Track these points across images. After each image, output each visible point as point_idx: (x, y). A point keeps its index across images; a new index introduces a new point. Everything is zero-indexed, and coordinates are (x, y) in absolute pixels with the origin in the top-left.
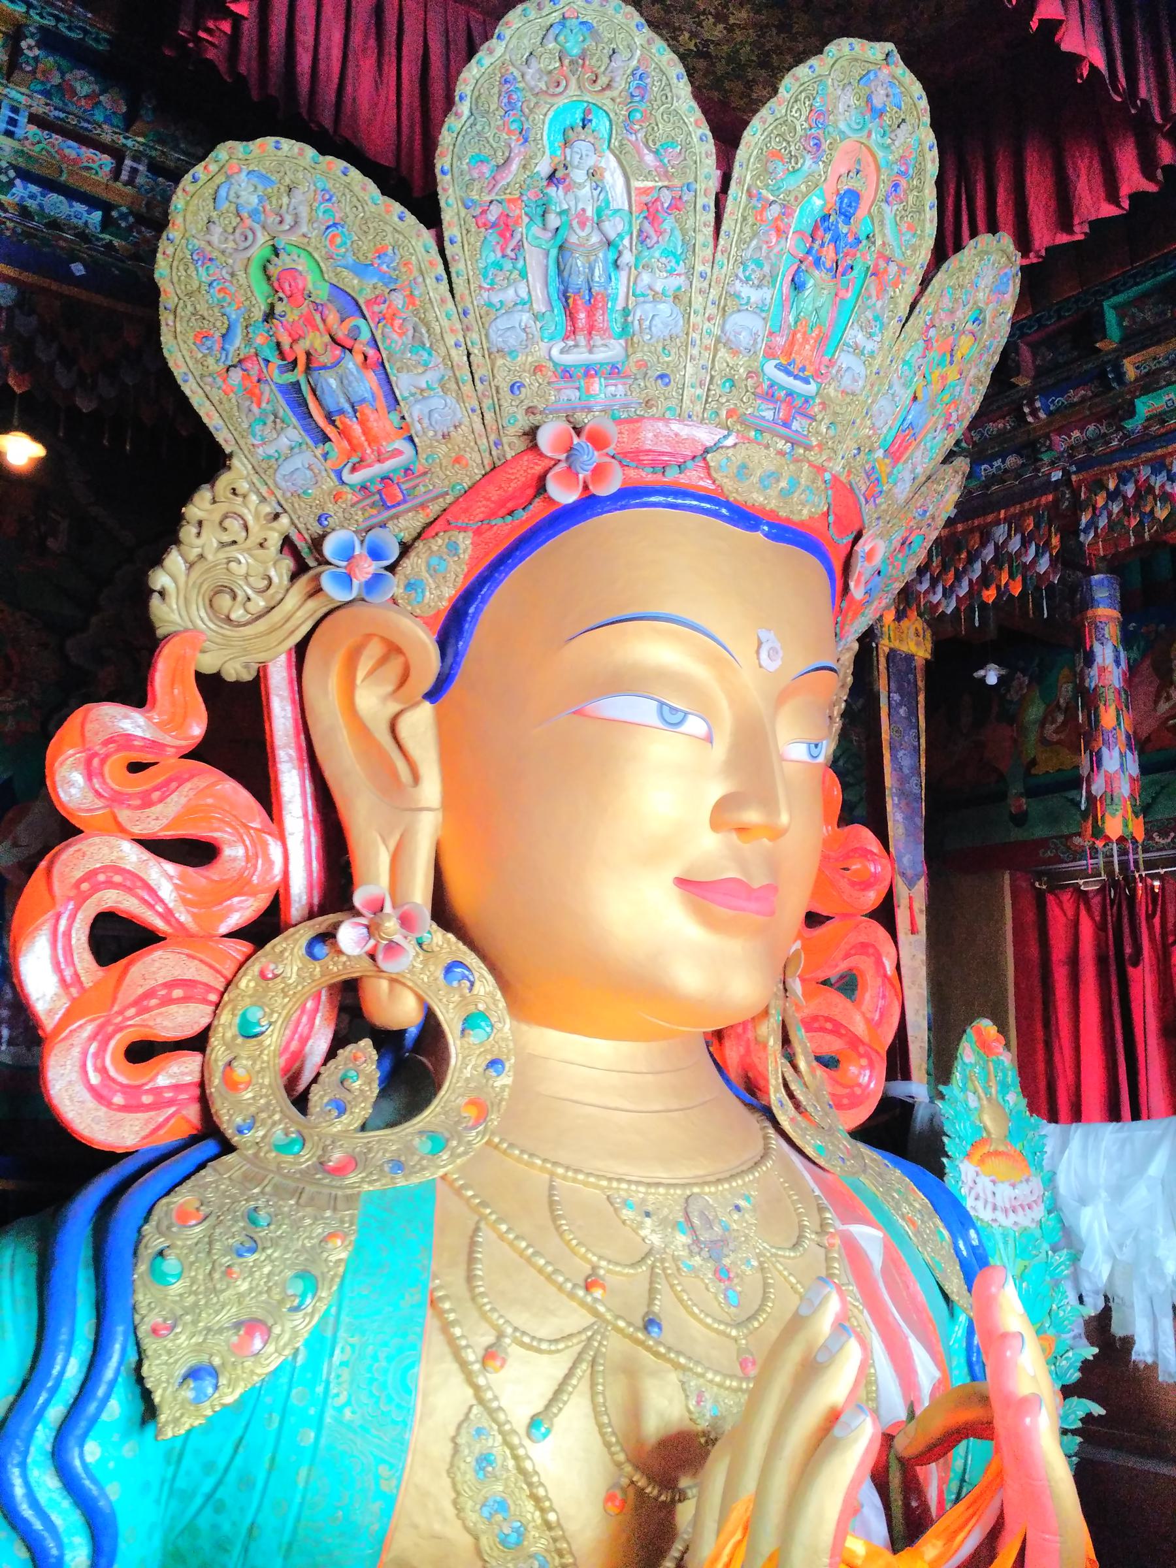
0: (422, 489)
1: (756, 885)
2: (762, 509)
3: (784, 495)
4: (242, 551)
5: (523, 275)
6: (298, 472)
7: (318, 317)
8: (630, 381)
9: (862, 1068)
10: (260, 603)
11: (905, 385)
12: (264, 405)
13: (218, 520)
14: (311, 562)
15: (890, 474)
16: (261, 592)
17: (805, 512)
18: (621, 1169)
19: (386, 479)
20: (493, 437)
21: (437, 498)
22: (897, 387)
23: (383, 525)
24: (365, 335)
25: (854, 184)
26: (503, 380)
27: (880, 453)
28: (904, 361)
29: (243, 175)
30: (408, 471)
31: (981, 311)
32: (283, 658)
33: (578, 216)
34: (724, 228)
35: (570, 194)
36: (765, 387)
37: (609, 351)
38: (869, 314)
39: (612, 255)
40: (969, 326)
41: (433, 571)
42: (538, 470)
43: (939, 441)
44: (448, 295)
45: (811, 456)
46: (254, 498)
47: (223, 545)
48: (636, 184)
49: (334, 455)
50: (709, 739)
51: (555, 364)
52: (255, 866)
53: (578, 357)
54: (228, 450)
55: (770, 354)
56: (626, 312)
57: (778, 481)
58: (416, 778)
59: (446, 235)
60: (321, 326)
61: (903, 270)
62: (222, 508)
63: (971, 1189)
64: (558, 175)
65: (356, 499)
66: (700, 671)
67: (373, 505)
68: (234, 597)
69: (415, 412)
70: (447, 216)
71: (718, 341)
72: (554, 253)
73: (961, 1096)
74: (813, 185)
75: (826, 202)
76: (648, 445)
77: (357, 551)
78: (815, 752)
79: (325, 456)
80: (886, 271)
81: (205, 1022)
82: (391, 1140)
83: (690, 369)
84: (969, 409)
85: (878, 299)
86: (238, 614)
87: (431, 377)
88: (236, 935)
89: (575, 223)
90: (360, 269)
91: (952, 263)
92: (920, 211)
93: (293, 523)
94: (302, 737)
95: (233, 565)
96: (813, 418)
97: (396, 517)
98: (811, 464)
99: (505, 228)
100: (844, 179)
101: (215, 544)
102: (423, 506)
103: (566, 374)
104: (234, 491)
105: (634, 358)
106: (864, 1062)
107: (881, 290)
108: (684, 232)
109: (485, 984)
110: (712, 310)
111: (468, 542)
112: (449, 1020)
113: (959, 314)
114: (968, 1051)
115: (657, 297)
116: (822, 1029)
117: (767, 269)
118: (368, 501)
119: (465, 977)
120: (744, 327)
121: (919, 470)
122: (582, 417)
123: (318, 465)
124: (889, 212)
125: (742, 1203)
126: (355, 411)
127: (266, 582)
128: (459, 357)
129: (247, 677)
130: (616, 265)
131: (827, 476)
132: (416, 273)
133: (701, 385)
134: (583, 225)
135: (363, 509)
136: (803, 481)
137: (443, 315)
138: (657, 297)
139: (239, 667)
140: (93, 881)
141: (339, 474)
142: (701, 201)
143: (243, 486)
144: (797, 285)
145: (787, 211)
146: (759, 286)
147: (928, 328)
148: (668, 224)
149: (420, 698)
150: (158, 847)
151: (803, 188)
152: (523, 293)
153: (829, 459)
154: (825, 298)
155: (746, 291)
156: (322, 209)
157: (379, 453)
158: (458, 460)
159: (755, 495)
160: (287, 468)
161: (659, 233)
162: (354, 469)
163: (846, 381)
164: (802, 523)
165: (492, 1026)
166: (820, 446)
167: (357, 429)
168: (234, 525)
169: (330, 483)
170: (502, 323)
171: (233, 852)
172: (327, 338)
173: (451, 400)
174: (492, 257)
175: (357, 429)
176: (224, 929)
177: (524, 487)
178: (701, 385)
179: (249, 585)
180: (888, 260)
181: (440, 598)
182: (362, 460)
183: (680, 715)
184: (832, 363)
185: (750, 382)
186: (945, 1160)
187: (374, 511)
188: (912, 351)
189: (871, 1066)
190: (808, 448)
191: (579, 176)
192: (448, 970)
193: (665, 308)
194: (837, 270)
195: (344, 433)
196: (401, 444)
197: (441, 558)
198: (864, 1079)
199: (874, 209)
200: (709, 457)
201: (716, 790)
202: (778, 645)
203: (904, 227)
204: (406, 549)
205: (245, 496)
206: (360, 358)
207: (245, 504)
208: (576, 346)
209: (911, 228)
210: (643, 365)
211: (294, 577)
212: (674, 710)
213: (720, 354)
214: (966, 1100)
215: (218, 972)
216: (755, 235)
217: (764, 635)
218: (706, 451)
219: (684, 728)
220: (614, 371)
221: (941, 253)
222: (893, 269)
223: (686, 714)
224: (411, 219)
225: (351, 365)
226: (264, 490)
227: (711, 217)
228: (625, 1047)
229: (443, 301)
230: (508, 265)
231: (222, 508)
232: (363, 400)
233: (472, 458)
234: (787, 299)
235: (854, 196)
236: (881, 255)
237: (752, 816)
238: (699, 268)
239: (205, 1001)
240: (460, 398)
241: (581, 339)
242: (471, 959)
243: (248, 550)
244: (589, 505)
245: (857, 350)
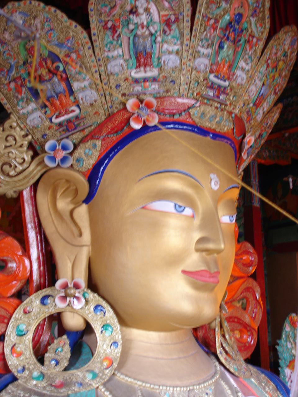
0: (82, 124)
1: (212, 272)
2: (210, 128)
3: (218, 123)
4: (14, 149)
5: (121, 46)
6: (35, 120)
7: (44, 64)
8: (160, 83)
9: (249, 336)
10: (20, 168)
11: (260, 80)
12: (23, 95)
13: (5, 137)
14: (39, 152)
15: (255, 112)
16: (21, 164)
17: (226, 129)
19: (69, 121)
20: (109, 105)
21: (88, 127)
22: (257, 81)
23: (67, 137)
24: (61, 68)
25: (241, 11)
26: (113, 84)
27: (251, 105)
28: (259, 72)
29: (18, 13)
30: (77, 118)
31: (286, 53)
32: (28, 189)
33: (141, 24)
34: (194, 28)
35: (138, 17)
36: (210, 84)
37: (152, 73)
38: (247, 56)
39: (153, 38)
40: (282, 58)
41: (87, 155)
42: (126, 116)
43: (272, 99)
44: (93, 54)
45: (227, 108)
46: (18, 129)
47: (6, 147)
48: (162, 13)
49: (49, 112)
50: (193, 217)
51: (132, 78)
52: (19, 269)
53: (141, 74)
54: (9, 111)
55: (211, 72)
56: (159, 58)
57: (216, 118)
58: (81, 235)
59: (92, 32)
60: (45, 66)
61: (258, 40)
62: (7, 133)
63: (289, 379)
64: (134, 10)
65: (57, 128)
66: (189, 191)
67: (63, 130)
68: (11, 166)
69: (80, 96)
70: (92, 26)
71: (192, 68)
72: (132, 38)
73: (285, 344)
74: (226, 12)
75: (230, 18)
76: (168, 107)
77: (57, 148)
78: (232, 219)
79: (46, 113)
80: (252, 41)
81: (3, 330)
82: (78, 373)
83: (182, 78)
84: (282, 87)
85: (250, 51)
86: (12, 173)
87: (86, 83)
88: (13, 296)
89: (140, 27)
90: (60, 45)
91: (275, 37)
92: (263, 19)
93: (33, 137)
94: (36, 219)
95: (11, 154)
96: (228, 94)
97: (73, 134)
98: (228, 112)
99: (114, 29)
100: (236, 9)
101: (4, 147)
102: (83, 130)
103: (137, 81)
104: (11, 127)
105: (161, 75)
106: (249, 333)
107: (251, 48)
108: (179, 30)
109: (110, 313)
110: (190, 57)
111: (100, 143)
112: (97, 327)
113: (279, 54)
114: (287, 326)
115: (170, 53)
116: (233, 321)
117: (210, 42)
118: (61, 129)
119: (101, 310)
120: (202, 63)
121: (265, 109)
122: (142, 97)
123: (43, 116)
124: (253, 20)
125: (208, 392)
126: (57, 97)
127: (22, 161)
128: (97, 76)
129: (15, 196)
130: (155, 42)
131: (233, 115)
132: (80, 46)
133: (187, 84)
134: (143, 28)
135: (60, 132)
136: (225, 118)
137: (91, 61)
138: (170, 53)
139: (12, 192)
141: (51, 120)
142: (186, 19)
143: (15, 124)
144: (221, 47)
145: (217, 21)
146: (207, 48)
147: (268, 60)
148: (174, 27)
149: (81, 203)
151: (222, 13)
152: (121, 53)
153: (234, 109)
154: (231, 52)
155: (203, 50)
156: (46, 24)
157: (66, 111)
158: (96, 113)
159: (207, 124)
160: (31, 117)
161: (170, 30)
162: (57, 117)
163: (239, 80)
164: (225, 133)
165: (113, 330)
166: (231, 104)
167: (58, 103)
168: (10, 139)
169: (47, 123)
170: (113, 63)
171: (13, 265)
172: (47, 70)
173: (94, 92)
174: (109, 40)
175: (58, 103)
176: (9, 295)
177: (121, 123)
178: (187, 84)
179: (16, 160)
180: (253, 37)
181: (89, 164)
182: (60, 113)
183: (182, 208)
184: (234, 74)
185: (205, 82)
186: (280, 369)
187: (62, 133)
188: (263, 69)
189: (252, 334)
190: (226, 105)
191: (141, 10)
192: (96, 307)
193: (173, 57)
194: (235, 42)
195: (53, 104)
196: (74, 108)
197: (90, 150)
198: (249, 340)
199: (247, 19)
200: (190, 111)
201: (197, 236)
202: (218, 180)
203: (258, 26)
204: (76, 147)
205: (15, 128)
206: (59, 77)
207: (15, 131)
208: (140, 71)
209: (261, 25)
210: (165, 77)
211: (33, 158)
212: (180, 207)
213: (193, 73)
214: (287, 345)
215: (7, 311)
216: (205, 30)
217: (212, 176)
218: (189, 108)
219: (184, 213)
220: (154, 80)
221: (273, 32)
223: (184, 208)
224: (79, 27)
225: (56, 80)
226: (22, 126)
227: (189, 24)
228: (162, 334)
229: (91, 56)
230: (115, 43)
231: (7, 133)
232: (60, 93)
233: (101, 111)
234: (217, 52)
235: (240, 15)
236: (250, 35)
237: (211, 246)
238: (185, 42)
239: (3, 322)
240: (98, 90)
241: (142, 69)
242: (104, 303)
243: (16, 149)
244: (146, 129)
245: (243, 69)
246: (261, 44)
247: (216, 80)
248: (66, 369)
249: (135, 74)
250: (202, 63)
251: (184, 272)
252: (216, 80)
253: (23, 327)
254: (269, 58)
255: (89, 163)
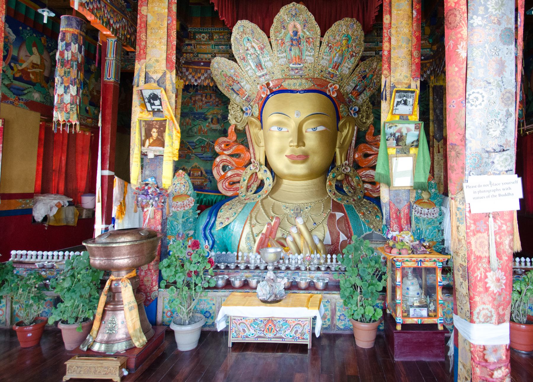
10: (240, 119)
18: (287, 201)
19: (247, 98)
55: (290, 63)
87: (245, 82)
103: (260, 77)
109: (269, 173)
140: (222, 161)
144: (291, 50)
150: (231, 155)
155: (280, 55)
163: (309, 61)
171: (242, 155)
180: (308, 38)
193: (270, 63)
220: (266, 74)
222: (311, 39)
242: (267, 169)
246: (318, 40)
247: (294, 66)
248: (254, 193)
249: (259, 74)
250: (283, 61)
251: (286, 156)
252: (294, 66)
253: (245, 178)
254: (329, 43)
255: (257, 113)
